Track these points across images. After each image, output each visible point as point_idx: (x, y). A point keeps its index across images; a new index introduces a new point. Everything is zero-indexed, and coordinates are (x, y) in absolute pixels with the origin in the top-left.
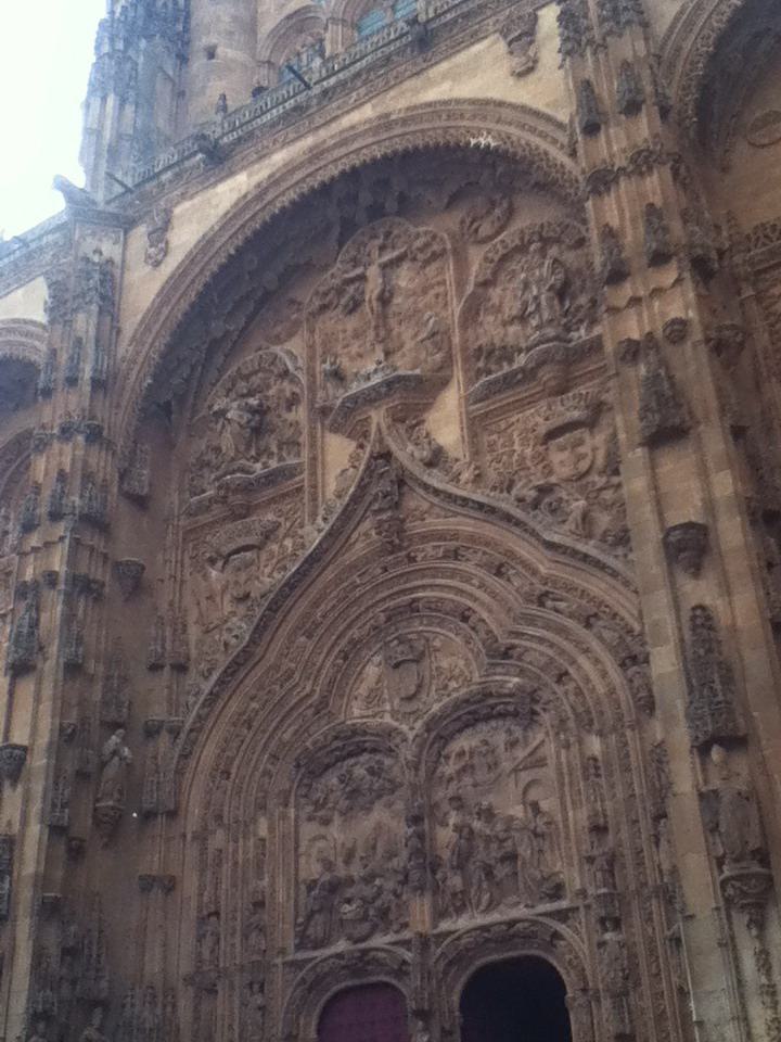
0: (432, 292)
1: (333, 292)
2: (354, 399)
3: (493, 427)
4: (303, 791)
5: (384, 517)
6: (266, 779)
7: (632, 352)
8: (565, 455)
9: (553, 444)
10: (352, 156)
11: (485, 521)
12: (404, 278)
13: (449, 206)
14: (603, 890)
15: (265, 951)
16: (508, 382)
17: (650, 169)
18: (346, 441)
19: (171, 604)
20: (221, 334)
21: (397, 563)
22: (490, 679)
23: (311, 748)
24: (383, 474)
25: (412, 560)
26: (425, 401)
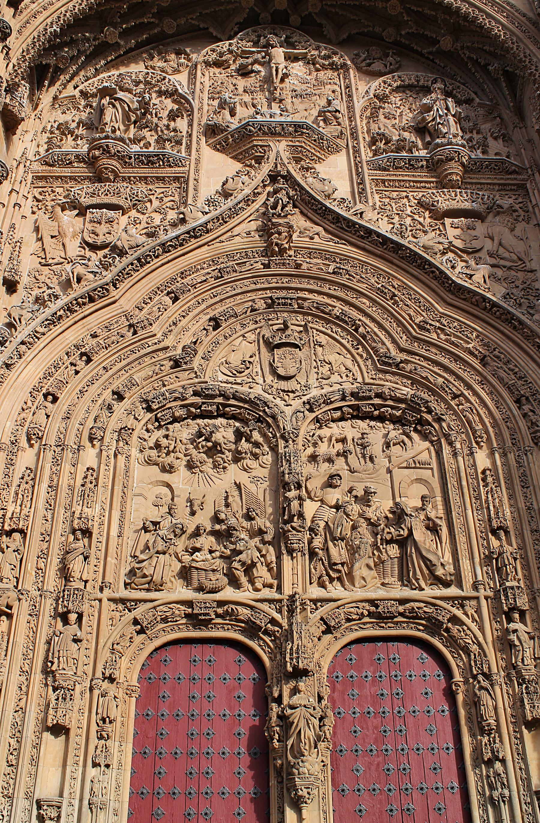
4: (146, 435)
6: (105, 412)
9: (448, 221)
14: (515, 584)
15: (86, 582)
19: (13, 227)
20: (114, 41)
23: (167, 393)
24: (281, 189)
25: (298, 266)
26: (318, 154)
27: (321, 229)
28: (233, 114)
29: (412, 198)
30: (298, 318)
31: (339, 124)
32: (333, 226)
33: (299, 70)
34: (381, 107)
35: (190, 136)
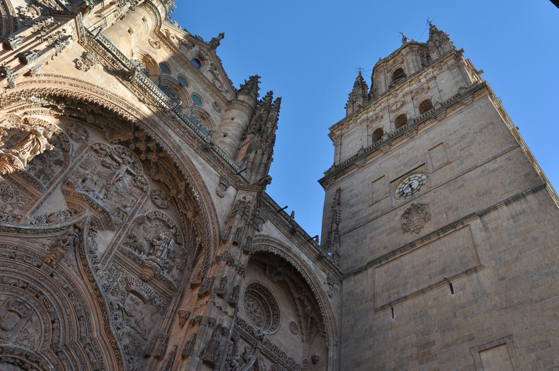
0: (132, 198)
1: (104, 152)
2: (88, 199)
3: (117, 264)
5: (61, 251)
7: (210, 323)
8: (131, 303)
9: (131, 295)
10: (161, 141)
11: (91, 294)
12: (128, 179)
13: (154, 180)
16: (136, 259)
17: (240, 274)
18: (64, 202)
21: (46, 270)
22: (42, 355)
24: (74, 235)
25: (52, 275)
27: (76, 264)
28: (84, 181)
29: (125, 274)
30: (32, 302)
31: (122, 219)
32: (82, 267)
33: (127, 180)
34: (145, 223)
35: (57, 178)
